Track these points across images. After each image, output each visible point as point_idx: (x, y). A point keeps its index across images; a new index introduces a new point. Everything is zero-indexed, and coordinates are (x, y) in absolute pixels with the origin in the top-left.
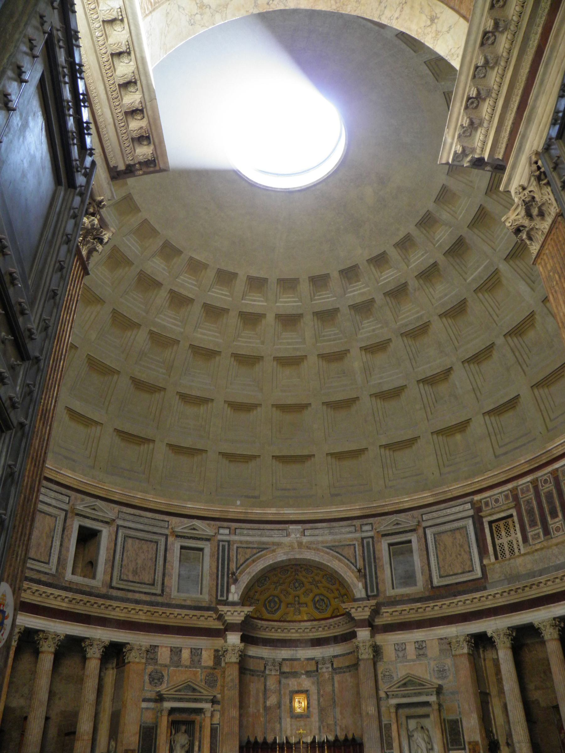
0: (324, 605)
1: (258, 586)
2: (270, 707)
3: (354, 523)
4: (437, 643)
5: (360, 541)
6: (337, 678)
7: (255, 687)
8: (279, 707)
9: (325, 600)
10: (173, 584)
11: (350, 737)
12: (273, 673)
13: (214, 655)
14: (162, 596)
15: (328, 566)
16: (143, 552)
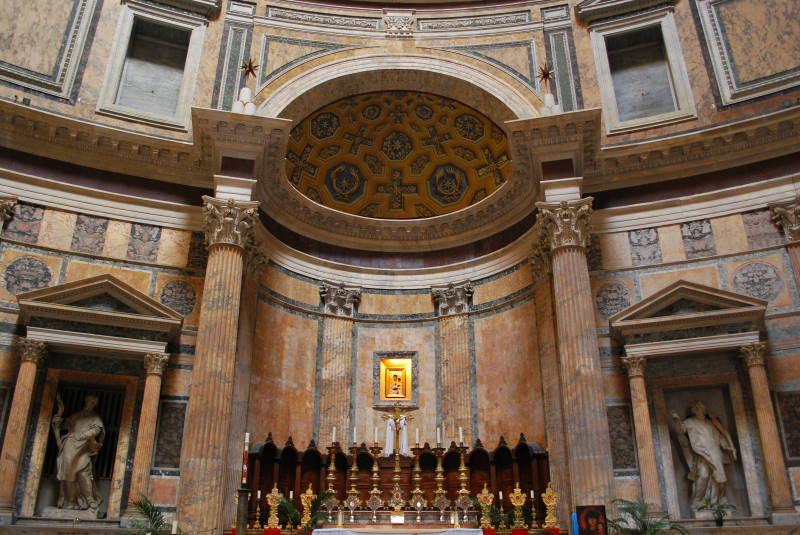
0: (454, 186)
1: (315, 134)
2: (329, 383)
3: (526, 8)
4: (741, 222)
5: (542, 36)
6: (480, 324)
7: (295, 334)
8: (351, 383)
9: (457, 175)
10: (105, 83)
11: (512, 445)
12: (340, 313)
13: (192, 244)
14: (74, 105)
15: (469, 83)
16: (36, 9)
